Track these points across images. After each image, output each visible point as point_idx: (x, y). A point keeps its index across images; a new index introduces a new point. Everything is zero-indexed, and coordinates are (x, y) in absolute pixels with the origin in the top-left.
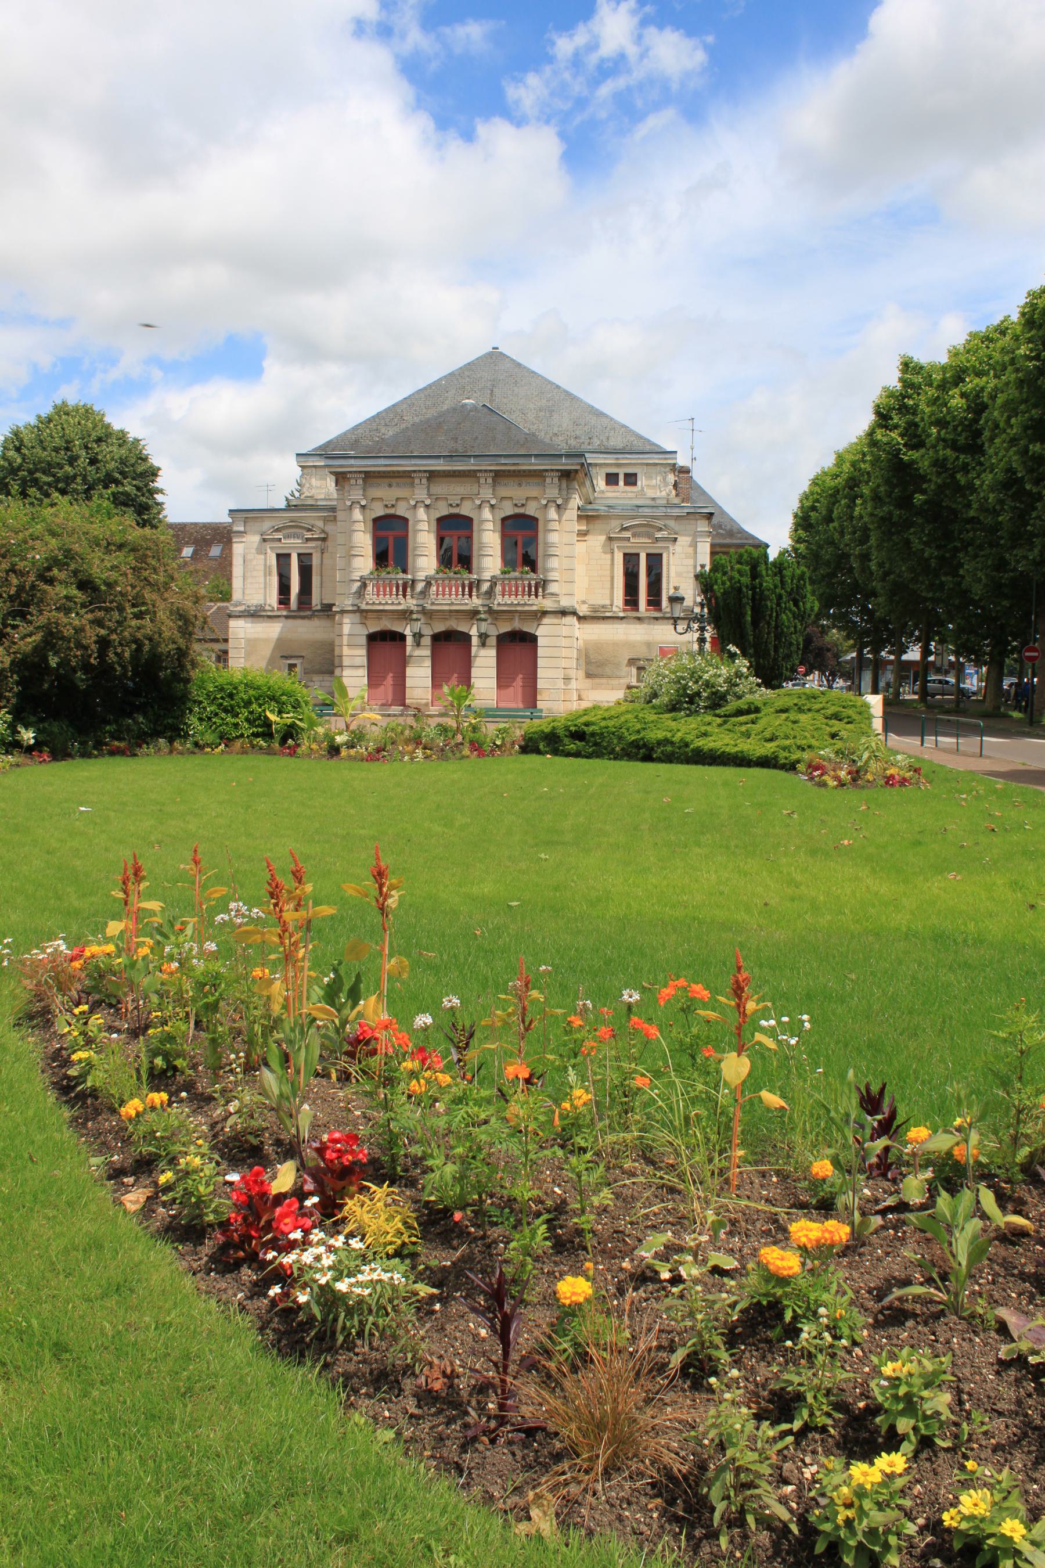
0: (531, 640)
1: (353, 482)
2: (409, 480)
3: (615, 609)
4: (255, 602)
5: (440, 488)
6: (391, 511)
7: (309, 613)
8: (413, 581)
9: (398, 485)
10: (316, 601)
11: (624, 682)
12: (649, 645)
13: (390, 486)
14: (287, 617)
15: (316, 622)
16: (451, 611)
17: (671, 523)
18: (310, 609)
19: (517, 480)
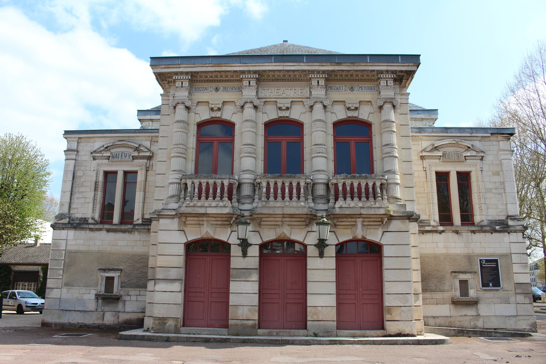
0: (374, 250)
1: (178, 84)
2: (237, 84)
3: (432, 223)
4: (79, 216)
5: (270, 92)
6: (217, 114)
7: (130, 226)
8: (240, 185)
9: (225, 89)
10: (137, 217)
11: (447, 295)
12: (469, 258)
13: (217, 90)
14: (108, 231)
15: (136, 236)
16: (284, 216)
17: (478, 144)
18: (131, 223)
19: (349, 84)
